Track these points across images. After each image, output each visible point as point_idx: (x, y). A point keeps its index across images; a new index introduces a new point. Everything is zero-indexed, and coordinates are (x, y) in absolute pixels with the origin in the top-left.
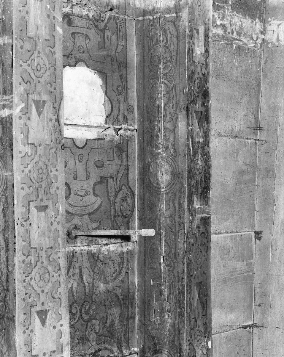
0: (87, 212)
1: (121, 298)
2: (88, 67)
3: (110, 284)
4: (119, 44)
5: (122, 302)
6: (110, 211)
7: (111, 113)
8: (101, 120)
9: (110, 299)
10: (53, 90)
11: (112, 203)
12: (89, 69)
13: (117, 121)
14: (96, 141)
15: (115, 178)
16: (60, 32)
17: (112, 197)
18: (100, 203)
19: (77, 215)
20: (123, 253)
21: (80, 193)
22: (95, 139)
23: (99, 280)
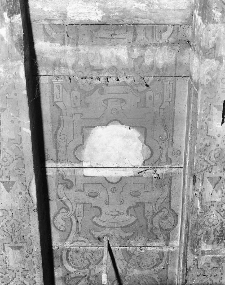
0: (120, 226)
2: (122, 124)
3: (146, 271)
4: (165, 101)
6: (147, 226)
7: (150, 157)
8: (139, 162)
10: (22, 174)
11: (149, 220)
12: (124, 126)
13: (158, 162)
14: (133, 177)
15: (153, 204)
16: (27, 132)
17: (150, 217)
18: (134, 220)
19: (109, 227)
20: (163, 253)
21: (113, 213)
22: (132, 177)
23: (133, 268)
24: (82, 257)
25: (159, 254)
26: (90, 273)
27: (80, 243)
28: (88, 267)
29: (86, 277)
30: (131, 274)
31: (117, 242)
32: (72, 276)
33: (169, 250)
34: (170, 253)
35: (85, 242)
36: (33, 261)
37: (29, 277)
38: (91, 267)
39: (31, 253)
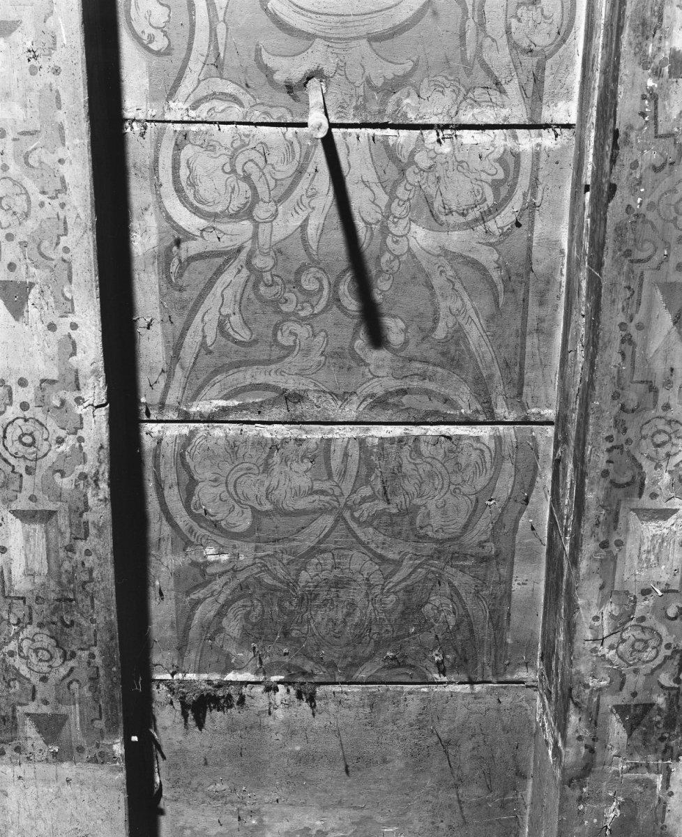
1: (495, 275)
5: (500, 287)
9: (450, 273)
11: (470, 8)
19: (325, 38)
23: (410, 220)
24: (228, 168)
25: (501, 161)
26: (255, 236)
27: (222, 108)
28: (246, 212)
29: (243, 256)
30: (400, 249)
31: (354, 104)
32: (192, 247)
33: (539, 145)
34: (543, 156)
35: (241, 105)
36: (57, 91)
37: (41, 163)
38: (261, 212)
39: (50, 55)
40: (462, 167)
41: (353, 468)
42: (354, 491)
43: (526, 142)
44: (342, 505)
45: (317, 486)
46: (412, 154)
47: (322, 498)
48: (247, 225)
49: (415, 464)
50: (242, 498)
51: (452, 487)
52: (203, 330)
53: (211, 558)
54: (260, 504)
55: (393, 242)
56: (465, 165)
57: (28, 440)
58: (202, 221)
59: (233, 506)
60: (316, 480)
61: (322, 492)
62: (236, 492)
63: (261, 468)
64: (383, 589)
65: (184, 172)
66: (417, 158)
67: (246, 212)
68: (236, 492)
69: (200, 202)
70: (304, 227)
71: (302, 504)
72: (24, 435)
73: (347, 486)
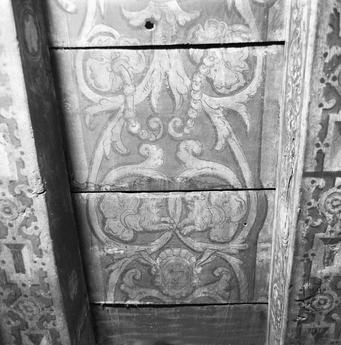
23: (202, 92)
24: (110, 70)
25: (247, 60)
26: (126, 102)
27: (105, 40)
28: (121, 91)
31: (171, 35)
35: (113, 36)
40: (227, 64)
41: (179, 211)
42: (180, 222)
43: (260, 51)
44: (175, 227)
45: (163, 219)
46: (202, 59)
47: (165, 225)
48: (120, 99)
49: (208, 208)
50: (128, 225)
51: (227, 219)
52: (104, 149)
53: (116, 252)
54: (137, 228)
55: (195, 103)
56: (229, 64)
57: (7, 210)
58: (99, 96)
59: (125, 229)
60: (162, 217)
61: (165, 222)
62: (125, 223)
63: (136, 212)
64: (196, 265)
65: (89, 72)
66: (205, 60)
67: (121, 91)
68: (125, 223)
69: (97, 87)
70: (149, 97)
71: (156, 228)
72: (6, 208)
73: (177, 220)
